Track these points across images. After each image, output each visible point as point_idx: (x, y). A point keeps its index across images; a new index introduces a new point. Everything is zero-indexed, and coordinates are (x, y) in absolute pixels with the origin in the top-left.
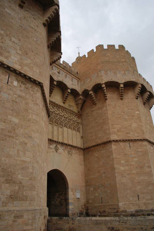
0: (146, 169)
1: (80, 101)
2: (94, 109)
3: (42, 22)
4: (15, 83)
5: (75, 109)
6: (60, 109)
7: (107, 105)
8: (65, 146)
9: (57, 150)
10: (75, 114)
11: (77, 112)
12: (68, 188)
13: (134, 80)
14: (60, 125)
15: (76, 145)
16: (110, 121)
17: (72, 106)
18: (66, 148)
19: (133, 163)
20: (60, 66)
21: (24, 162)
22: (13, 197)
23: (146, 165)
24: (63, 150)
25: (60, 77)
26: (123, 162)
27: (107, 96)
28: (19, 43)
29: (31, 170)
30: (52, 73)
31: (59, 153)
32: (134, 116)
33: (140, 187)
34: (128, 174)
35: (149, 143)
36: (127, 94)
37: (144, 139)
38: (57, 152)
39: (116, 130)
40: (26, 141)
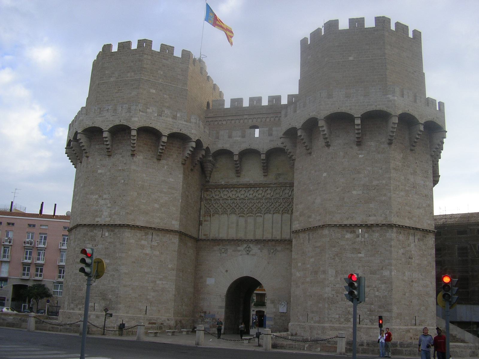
3: (130, 153)
4: (107, 234)
9: (248, 252)
13: (314, 113)
19: (309, 266)
21: (113, 287)
23: (322, 269)
28: (109, 196)
31: (253, 255)
33: (311, 303)
37: (323, 225)
38: (248, 254)
40: (114, 274)
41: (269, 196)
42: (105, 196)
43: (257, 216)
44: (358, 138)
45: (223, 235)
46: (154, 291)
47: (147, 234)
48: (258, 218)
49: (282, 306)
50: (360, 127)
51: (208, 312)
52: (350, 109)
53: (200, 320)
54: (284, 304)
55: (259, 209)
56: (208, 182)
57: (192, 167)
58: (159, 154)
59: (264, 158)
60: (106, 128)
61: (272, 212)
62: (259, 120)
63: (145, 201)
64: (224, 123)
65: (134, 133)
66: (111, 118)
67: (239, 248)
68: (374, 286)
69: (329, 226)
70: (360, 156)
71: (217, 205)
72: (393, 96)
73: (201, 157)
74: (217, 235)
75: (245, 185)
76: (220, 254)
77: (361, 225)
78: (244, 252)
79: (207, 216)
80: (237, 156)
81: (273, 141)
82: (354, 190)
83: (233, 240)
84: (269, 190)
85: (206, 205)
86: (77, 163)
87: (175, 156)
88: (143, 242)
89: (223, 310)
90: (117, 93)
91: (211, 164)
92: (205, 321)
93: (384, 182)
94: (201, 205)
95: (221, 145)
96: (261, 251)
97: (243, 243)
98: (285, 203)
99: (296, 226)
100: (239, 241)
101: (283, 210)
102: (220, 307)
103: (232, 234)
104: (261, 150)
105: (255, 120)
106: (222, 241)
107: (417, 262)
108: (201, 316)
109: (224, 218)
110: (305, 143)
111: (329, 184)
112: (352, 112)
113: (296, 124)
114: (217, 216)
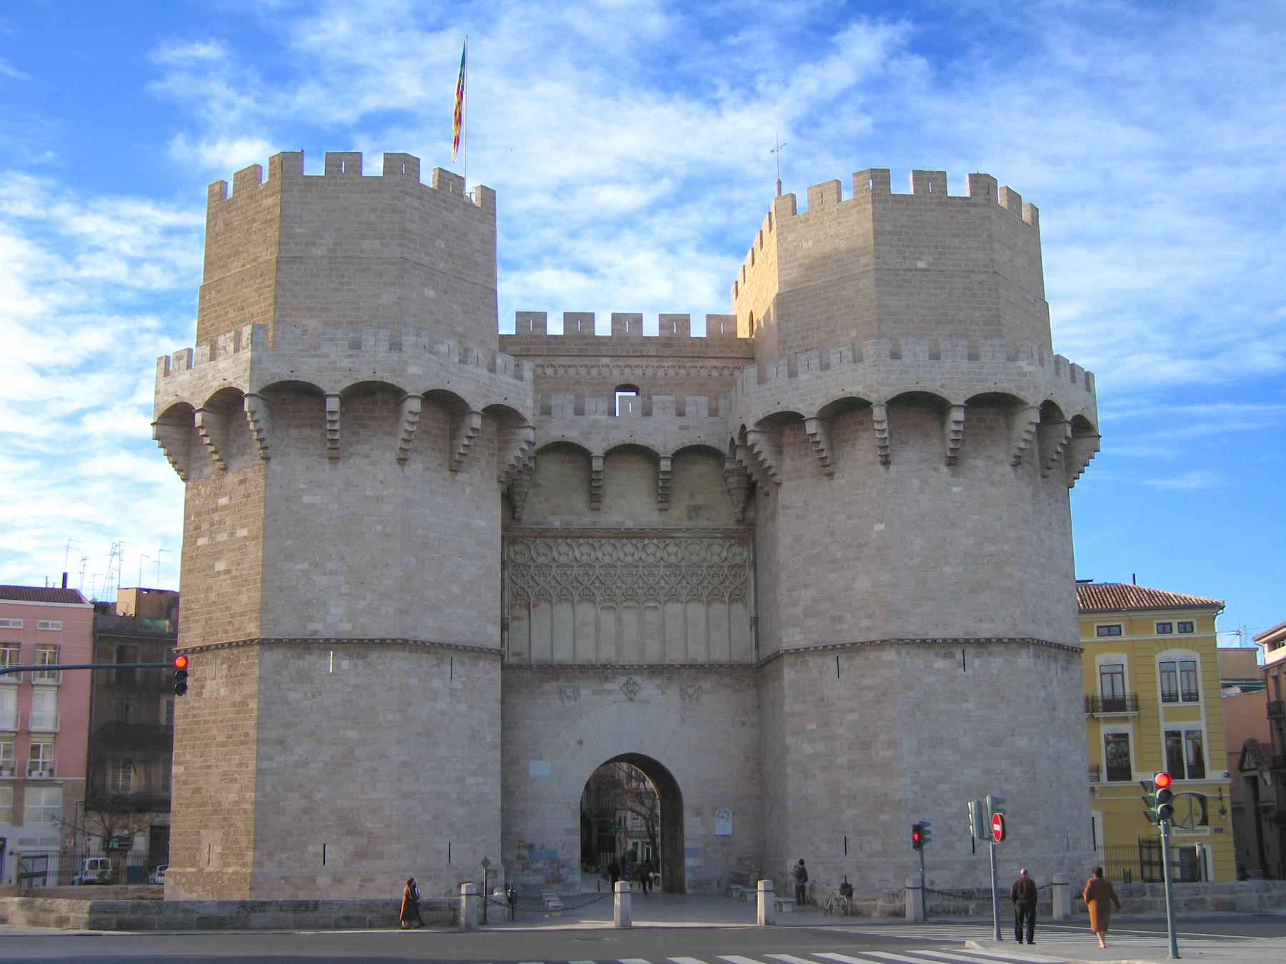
0: (881, 753)
3: (391, 456)
4: (345, 664)
5: (723, 514)
7: (780, 511)
12: (681, 806)
16: (783, 576)
19: (841, 730)
22: (360, 854)
24: (659, 687)
26: (811, 726)
27: (775, 474)
29: (387, 812)
31: (643, 702)
32: (866, 545)
33: (855, 812)
34: (824, 769)
35: (914, 651)
36: (853, 446)
38: (631, 699)
39: (798, 610)
41: (672, 559)
42: (330, 566)
44: (952, 449)
45: (563, 654)
46: (462, 804)
47: (440, 660)
48: (648, 613)
50: (961, 428)
51: (538, 846)
52: (942, 386)
55: (652, 591)
56: (519, 520)
58: (457, 457)
60: (332, 388)
62: (638, 372)
63: (432, 579)
64: (550, 371)
65: (414, 405)
66: (346, 363)
67: (609, 686)
68: (998, 770)
69: (900, 643)
70: (955, 489)
72: (1030, 364)
74: (548, 655)
77: (967, 641)
81: (687, 428)
82: (946, 563)
86: (188, 467)
87: (483, 463)
88: (436, 683)
89: (577, 838)
90: (336, 290)
92: (533, 867)
93: (1006, 547)
95: (555, 431)
96: (663, 693)
99: (792, 638)
102: (569, 832)
103: (587, 653)
104: (660, 450)
105: (627, 370)
107: (1062, 715)
108: (520, 857)
109: (563, 612)
110: (822, 450)
111: (870, 544)
112: (944, 393)
113: (801, 406)
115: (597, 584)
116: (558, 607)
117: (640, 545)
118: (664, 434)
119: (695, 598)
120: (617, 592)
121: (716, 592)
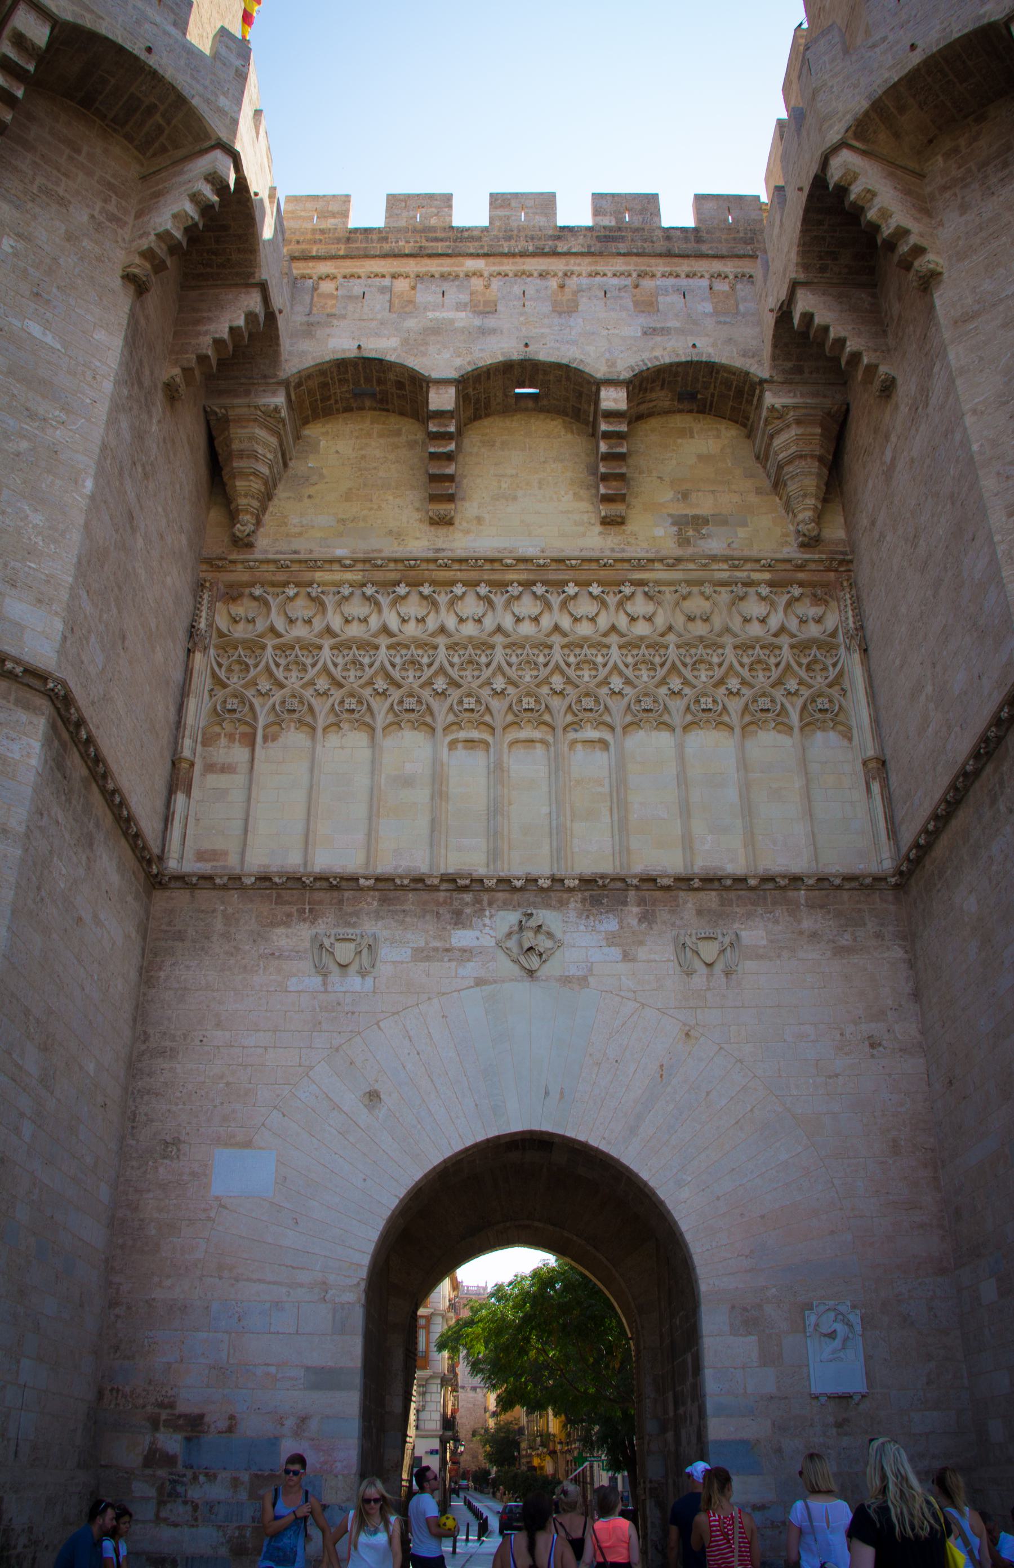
1: (786, 441)
2: (893, 438)
5: (766, 532)
6: (571, 589)
8: (641, 902)
9: (530, 955)
10: (767, 576)
11: (791, 551)
14: (577, 725)
15: (798, 865)
17: (722, 521)
18: (643, 918)
20: (555, 254)
24: (612, 940)
25: (493, 331)
30: (405, 342)
31: (566, 980)
38: (531, 973)
43: (574, 742)
45: (338, 854)
49: (837, 1343)
51: (216, 1420)
53: (152, 1493)
54: (838, 1326)
55: (588, 703)
57: (177, 371)
59: (623, 406)
61: (677, 719)
67: (462, 938)
71: (294, 674)
73: (241, 322)
75: (488, 566)
76: (319, 979)
78: (505, 966)
79: (223, 741)
80: (452, 391)
81: (664, 331)
83: (419, 882)
84: (639, 598)
85: (222, 674)
91: (273, 441)
92: (194, 1493)
94: (188, 671)
95: (340, 342)
96: (626, 957)
97: (490, 904)
98: (750, 670)
100: (465, 889)
101: (746, 708)
104: (599, 370)
106: (333, 888)
108: (155, 1458)
109: (346, 750)
114: (294, 738)
115: (440, 684)
116: (333, 740)
117: (555, 600)
118: (608, 339)
119: (705, 715)
120: (495, 704)
121: (764, 703)
